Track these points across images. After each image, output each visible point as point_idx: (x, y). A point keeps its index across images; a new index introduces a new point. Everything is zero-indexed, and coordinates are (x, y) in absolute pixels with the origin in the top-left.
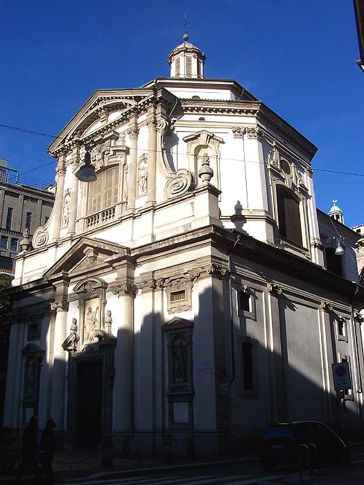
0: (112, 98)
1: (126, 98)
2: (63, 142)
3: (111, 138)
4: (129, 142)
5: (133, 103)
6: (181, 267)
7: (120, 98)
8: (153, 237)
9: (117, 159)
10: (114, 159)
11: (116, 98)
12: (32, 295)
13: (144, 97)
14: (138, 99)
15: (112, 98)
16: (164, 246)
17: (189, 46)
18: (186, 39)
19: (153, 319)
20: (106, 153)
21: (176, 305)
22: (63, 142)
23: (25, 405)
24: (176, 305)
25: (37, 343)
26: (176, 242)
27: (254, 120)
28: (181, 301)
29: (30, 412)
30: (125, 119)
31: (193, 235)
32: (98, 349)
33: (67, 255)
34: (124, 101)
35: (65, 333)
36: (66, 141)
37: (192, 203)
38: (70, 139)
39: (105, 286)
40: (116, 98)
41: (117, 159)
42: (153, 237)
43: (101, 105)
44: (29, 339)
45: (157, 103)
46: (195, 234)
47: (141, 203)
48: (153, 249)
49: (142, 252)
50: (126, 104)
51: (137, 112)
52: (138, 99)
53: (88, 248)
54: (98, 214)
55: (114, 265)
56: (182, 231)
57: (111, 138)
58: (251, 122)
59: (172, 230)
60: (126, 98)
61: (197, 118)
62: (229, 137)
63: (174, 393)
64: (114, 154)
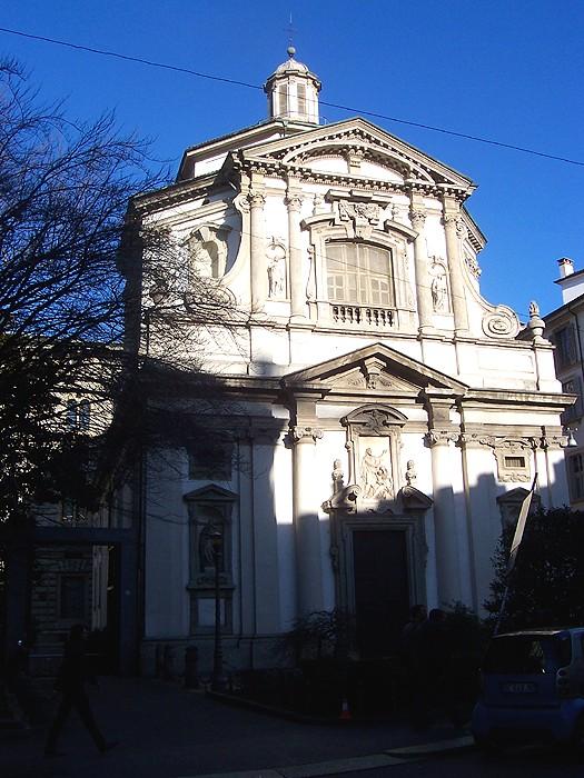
0: (386, 146)
4: (403, 220)
5: (431, 182)
6: (520, 429)
7: (401, 154)
10: (384, 238)
11: (393, 150)
13: (449, 182)
14: (438, 178)
15: (386, 146)
16: (513, 399)
17: (294, 65)
18: (291, 55)
22: (278, 155)
23: (194, 593)
24: (510, 473)
26: (530, 400)
29: (207, 611)
30: (407, 190)
32: (401, 513)
33: (343, 359)
34: (412, 166)
35: (306, 478)
36: (291, 155)
38: (293, 159)
40: (393, 150)
43: (366, 145)
49: (481, 396)
50: (416, 172)
51: (427, 191)
52: (438, 178)
53: (374, 359)
55: (432, 400)
64: (387, 228)
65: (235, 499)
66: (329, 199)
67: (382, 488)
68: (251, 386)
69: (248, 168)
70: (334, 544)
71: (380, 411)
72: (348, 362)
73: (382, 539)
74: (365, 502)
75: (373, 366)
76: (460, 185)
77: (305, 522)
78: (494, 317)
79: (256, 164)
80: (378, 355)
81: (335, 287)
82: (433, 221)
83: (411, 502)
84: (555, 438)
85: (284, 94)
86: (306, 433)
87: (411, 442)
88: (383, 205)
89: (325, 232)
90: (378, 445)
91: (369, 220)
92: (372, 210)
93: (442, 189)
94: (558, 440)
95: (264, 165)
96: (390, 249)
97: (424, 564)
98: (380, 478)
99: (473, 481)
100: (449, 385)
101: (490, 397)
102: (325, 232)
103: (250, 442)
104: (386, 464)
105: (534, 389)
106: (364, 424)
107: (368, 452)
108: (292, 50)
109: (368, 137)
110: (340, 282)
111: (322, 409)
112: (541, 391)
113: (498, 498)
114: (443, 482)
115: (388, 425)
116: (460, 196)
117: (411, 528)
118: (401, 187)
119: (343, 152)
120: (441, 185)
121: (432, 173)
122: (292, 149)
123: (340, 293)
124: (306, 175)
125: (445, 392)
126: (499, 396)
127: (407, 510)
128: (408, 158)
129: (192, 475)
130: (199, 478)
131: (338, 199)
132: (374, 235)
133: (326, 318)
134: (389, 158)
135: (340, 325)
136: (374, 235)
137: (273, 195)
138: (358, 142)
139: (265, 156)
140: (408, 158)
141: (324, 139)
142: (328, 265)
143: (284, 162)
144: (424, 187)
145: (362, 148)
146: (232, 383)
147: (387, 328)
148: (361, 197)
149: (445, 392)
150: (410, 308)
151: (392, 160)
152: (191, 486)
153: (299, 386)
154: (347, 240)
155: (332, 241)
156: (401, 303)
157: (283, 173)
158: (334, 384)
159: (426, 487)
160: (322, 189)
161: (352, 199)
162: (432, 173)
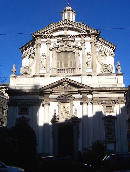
0: (73, 25)
1: (82, 28)
2: (44, 33)
3: (72, 41)
4: (80, 45)
5: (86, 33)
6: (111, 98)
7: (78, 27)
8: (99, 86)
9: (74, 50)
11: (75, 26)
12: (27, 95)
14: (88, 31)
16: (107, 90)
18: (68, 5)
19: (99, 114)
20: (70, 46)
21: (108, 111)
22: (44, 33)
24: (108, 111)
25: (27, 116)
26: (113, 90)
27: (112, 51)
28: (110, 110)
30: (80, 36)
31: (120, 89)
34: (81, 29)
36: (46, 33)
37: (115, 78)
38: (48, 33)
39: (74, 99)
40: (75, 26)
41: (74, 50)
42: (99, 86)
43: (68, 26)
44: (20, 114)
45: (95, 36)
46: (121, 89)
47: (89, 70)
48: (102, 90)
49: (97, 90)
50: (82, 31)
51: (86, 35)
52: (88, 31)
53: (65, 82)
54: (64, 70)
55: (81, 92)
56: (111, 86)
57: (72, 41)
58: (112, 51)
59: (108, 84)
60: (82, 28)
61: (101, 45)
62: (108, 54)
63: (108, 141)
64: (73, 47)
65: (29, 120)
66: (58, 42)
67: (67, 116)
68: (32, 92)
69: (36, 37)
70: (53, 131)
71: (67, 96)
72: (57, 84)
73: (67, 130)
74: (62, 120)
75: (65, 84)
76: (95, 32)
77: (46, 125)
78: (105, 67)
79: (38, 36)
80: (66, 81)
81: (60, 64)
82: (88, 44)
83: (75, 119)
84: (122, 100)
85: (65, 14)
86: (45, 102)
87: (77, 104)
88: (73, 41)
89: (56, 50)
90: (67, 105)
91: (68, 46)
92: (69, 43)
93: (90, 34)
94: (123, 101)
95: (40, 36)
96: (75, 52)
97: (78, 137)
98: (67, 113)
99: (94, 114)
100: (86, 87)
101: (100, 90)
102: (56, 50)
103: (33, 105)
104: (69, 110)
105: (115, 86)
106: (62, 99)
107: (64, 107)
108: (69, 4)
109: (69, 24)
110: (61, 62)
111: (51, 96)
112: (118, 87)
113: (103, 118)
114: (85, 114)
115: (69, 99)
116: (95, 35)
117: (75, 126)
118: (78, 35)
119: (62, 29)
120: (89, 33)
121: (86, 30)
122: (47, 31)
123: (61, 66)
124: (52, 37)
125: (84, 89)
126: (102, 89)
127: (73, 122)
128: (80, 28)
129: (20, 114)
130: (21, 115)
131: (60, 41)
132: (70, 49)
133: (55, 73)
134: (72, 28)
135: (59, 74)
136: (70, 49)
137: (43, 43)
138: (66, 26)
139: (40, 34)
140: (80, 28)
141: (56, 26)
142: (58, 58)
143: (45, 34)
144: (84, 34)
145: (67, 27)
146: (27, 91)
147: (72, 74)
148: (65, 39)
149: (84, 89)
150: (80, 67)
151: (73, 28)
152: (18, 116)
153: (43, 91)
154: (63, 52)
155: (59, 52)
156: (77, 66)
157: (46, 37)
158: (54, 90)
159: (80, 116)
160: (56, 40)
161: (64, 41)
162: (86, 30)
